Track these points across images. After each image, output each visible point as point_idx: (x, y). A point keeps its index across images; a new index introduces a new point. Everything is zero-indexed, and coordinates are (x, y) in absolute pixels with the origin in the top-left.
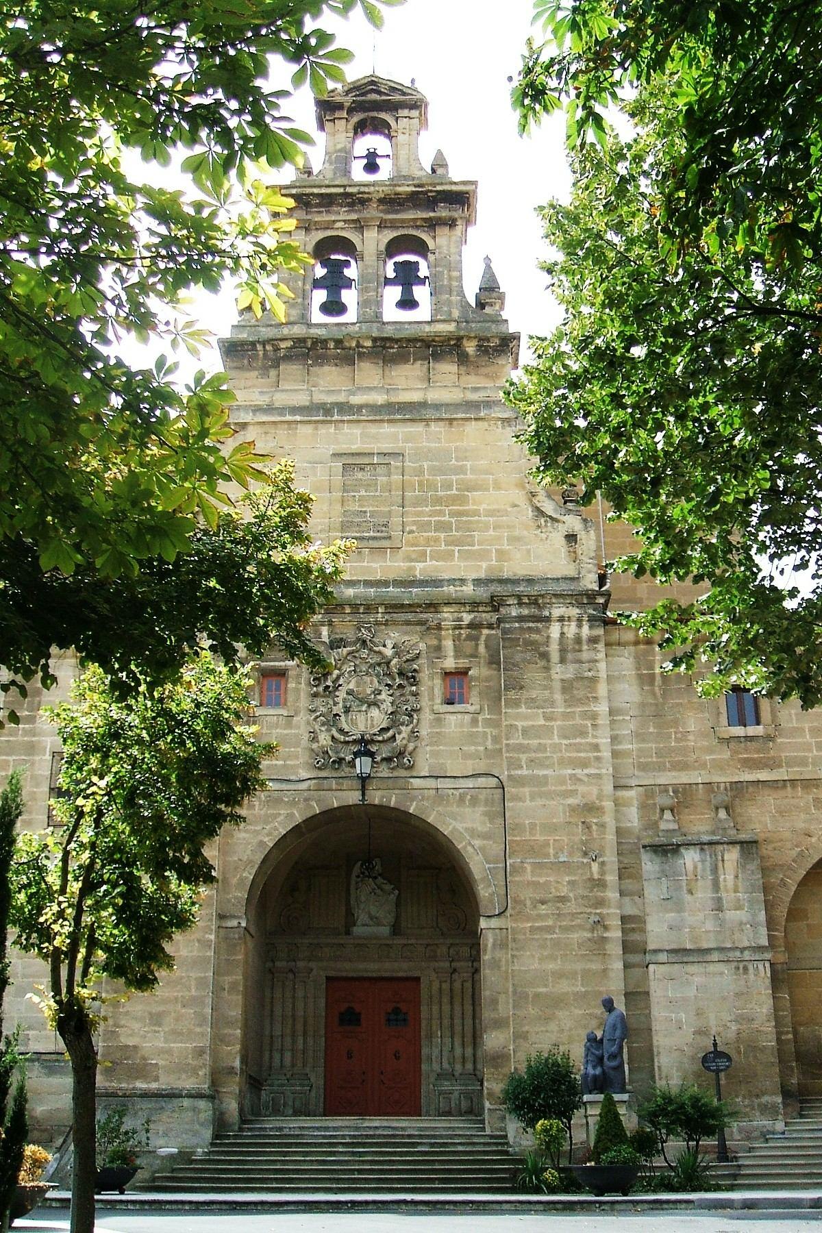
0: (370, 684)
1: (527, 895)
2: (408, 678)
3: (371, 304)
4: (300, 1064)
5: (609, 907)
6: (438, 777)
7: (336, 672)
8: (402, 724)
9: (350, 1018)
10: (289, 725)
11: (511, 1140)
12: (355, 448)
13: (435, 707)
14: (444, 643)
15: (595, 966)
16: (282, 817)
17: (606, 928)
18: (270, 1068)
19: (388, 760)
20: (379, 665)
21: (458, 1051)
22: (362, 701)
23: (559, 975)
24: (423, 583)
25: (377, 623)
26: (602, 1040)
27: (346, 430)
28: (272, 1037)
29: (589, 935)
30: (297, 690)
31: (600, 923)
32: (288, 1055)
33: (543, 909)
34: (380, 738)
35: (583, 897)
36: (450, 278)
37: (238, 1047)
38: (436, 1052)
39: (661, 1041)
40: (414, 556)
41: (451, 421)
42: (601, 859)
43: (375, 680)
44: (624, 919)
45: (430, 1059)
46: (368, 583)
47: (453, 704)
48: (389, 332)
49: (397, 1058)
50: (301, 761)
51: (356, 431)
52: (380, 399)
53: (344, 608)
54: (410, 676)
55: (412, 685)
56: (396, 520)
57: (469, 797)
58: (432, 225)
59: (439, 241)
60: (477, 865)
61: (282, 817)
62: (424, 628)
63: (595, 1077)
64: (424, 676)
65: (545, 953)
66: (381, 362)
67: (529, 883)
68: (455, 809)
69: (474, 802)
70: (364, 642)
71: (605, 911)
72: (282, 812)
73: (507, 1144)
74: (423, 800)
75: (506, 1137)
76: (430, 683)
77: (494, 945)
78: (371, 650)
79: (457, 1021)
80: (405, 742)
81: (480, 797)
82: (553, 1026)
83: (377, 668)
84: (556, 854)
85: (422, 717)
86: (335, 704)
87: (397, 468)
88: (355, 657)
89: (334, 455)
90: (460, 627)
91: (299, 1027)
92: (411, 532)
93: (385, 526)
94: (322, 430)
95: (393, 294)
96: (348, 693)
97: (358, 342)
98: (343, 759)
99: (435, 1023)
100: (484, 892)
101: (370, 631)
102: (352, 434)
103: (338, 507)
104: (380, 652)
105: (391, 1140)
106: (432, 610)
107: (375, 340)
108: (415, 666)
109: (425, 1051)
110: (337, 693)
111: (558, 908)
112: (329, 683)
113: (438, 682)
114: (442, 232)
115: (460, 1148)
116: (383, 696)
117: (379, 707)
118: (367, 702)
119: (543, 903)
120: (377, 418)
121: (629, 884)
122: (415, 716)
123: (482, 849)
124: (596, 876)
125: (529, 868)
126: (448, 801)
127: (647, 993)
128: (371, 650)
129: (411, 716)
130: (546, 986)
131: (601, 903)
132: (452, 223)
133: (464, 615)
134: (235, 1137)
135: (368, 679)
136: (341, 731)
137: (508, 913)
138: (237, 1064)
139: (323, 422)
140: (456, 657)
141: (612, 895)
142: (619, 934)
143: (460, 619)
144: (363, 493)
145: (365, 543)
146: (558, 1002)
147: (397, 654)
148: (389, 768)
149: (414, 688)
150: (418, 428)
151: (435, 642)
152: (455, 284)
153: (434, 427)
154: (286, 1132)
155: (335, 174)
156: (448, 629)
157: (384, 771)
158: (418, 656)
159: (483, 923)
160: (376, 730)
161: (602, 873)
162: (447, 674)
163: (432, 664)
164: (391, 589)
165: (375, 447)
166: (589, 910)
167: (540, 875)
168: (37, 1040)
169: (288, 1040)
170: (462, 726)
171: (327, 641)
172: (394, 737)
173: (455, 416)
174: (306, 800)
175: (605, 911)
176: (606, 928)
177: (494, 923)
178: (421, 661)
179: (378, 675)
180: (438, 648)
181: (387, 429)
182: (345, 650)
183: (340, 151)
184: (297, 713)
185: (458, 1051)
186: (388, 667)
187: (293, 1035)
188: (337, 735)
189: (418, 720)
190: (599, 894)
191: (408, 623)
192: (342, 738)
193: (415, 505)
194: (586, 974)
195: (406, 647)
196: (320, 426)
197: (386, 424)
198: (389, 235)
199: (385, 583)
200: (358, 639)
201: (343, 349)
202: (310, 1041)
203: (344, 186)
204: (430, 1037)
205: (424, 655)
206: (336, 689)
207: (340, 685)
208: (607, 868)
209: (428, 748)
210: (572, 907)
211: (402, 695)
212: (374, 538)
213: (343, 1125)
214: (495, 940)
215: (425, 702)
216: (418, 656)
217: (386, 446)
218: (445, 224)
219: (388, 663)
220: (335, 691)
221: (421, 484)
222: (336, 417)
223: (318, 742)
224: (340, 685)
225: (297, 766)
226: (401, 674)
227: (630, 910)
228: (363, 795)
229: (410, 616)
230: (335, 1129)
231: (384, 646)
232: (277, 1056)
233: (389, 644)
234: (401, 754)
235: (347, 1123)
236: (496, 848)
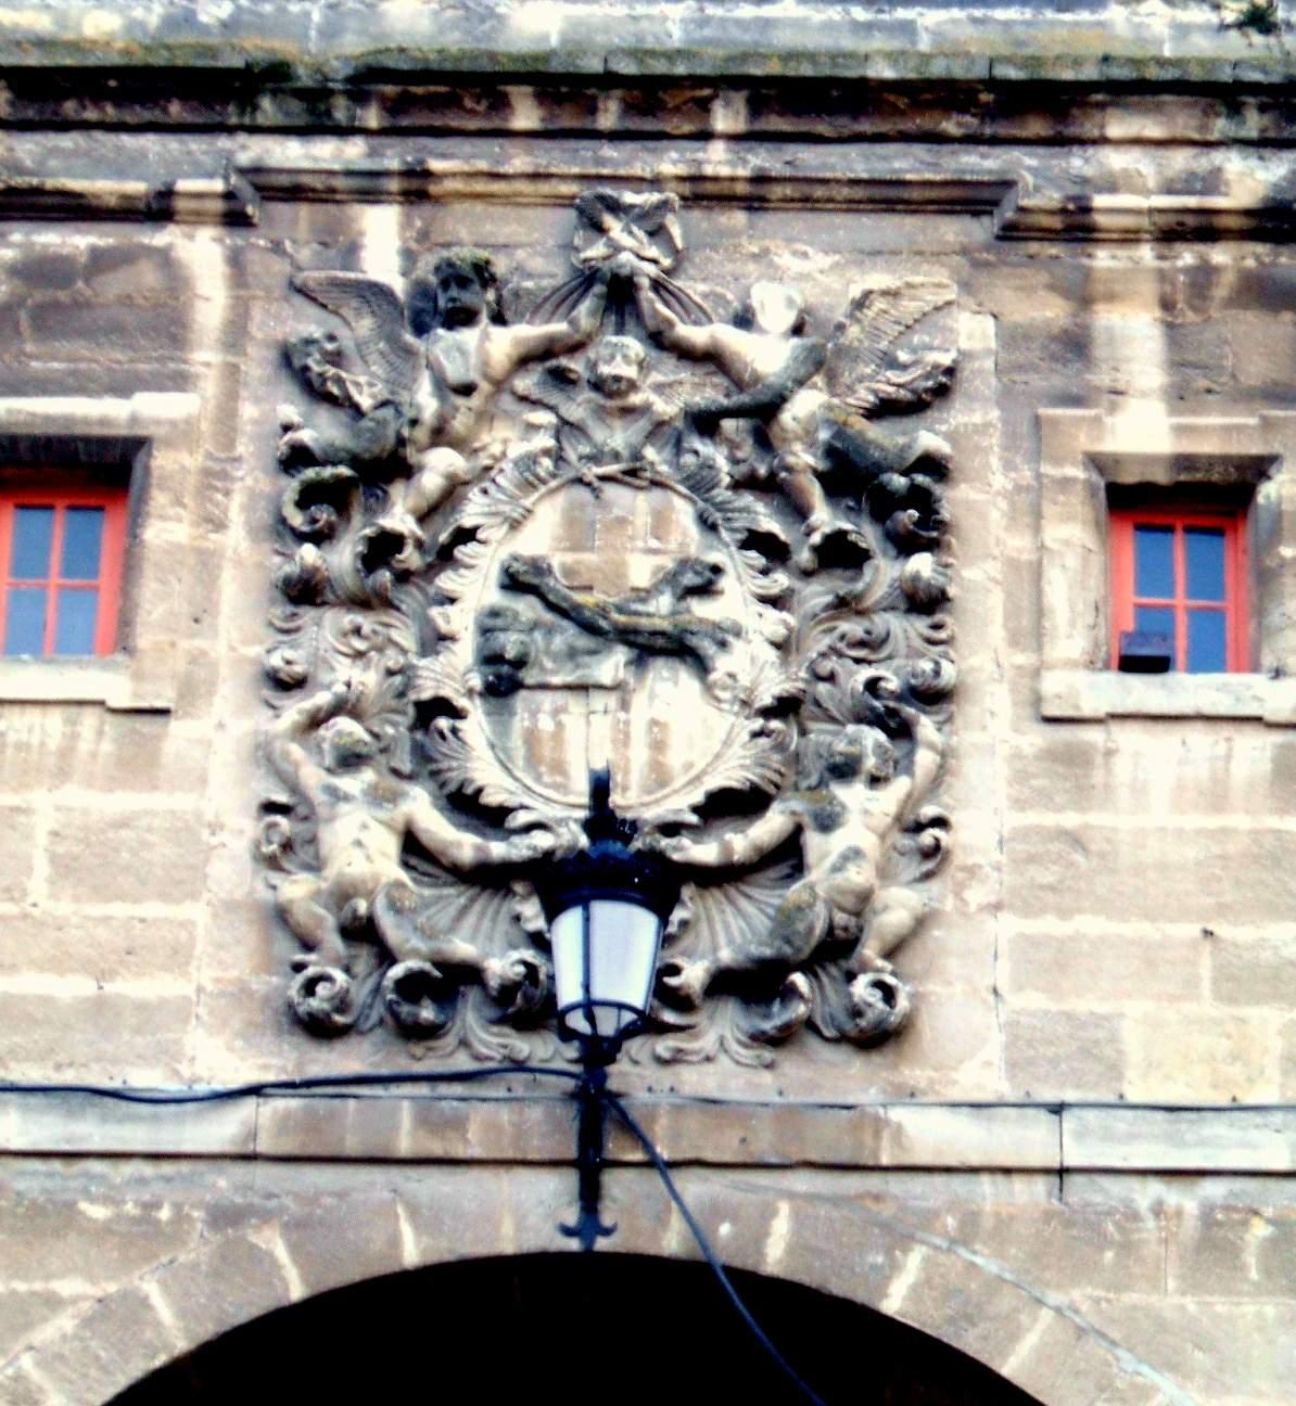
2: (881, 505)
6: (1007, 1171)
7: (438, 466)
8: (844, 770)
10: (138, 767)
13: (1052, 683)
14: (1107, 318)
16: (66, 1322)
25: (703, 194)
30: (206, 564)
34: (704, 852)
43: (683, 512)
47: (1158, 665)
50: (206, 976)
53: (501, 104)
55: (905, 545)
57: (1260, 1230)
61: (66, 1322)
62: (979, 230)
68: (1173, 1300)
72: (66, 1287)
76: (1019, 544)
78: (659, 340)
80: (858, 876)
83: (705, 448)
86: (436, 641)
88: (562, 378)
90: (1202, 228)
96: (514, 583)
98: (469, 974)
101: (657, 233)
104: (711, 359)
106: (1037, 127)
110: (446, 581)
112: (399, 517)
117: (701, 666)
118: (626, 636)
122: (926, 726)
126: (1127, 1247)
128: (659, 340)
129: (902, 731)
133: (1233, 163)
135: (637, 505)
136: (466, 805)
140: (1180, 396)
143: (1212, 182)
147: (819, 364)
148: (759, 1039)
149: (922, 564)
151: (1052, 311)
156: (1129, 238)
160: (680, 803)
163: (1036, 437)
170: (1216, 796)
174: (225, 1217)
179: (699, 484)
180: (1075, 345)
182: (498, 344)
184: (193, 691)
188: (440, 828)
189: (944, 754)
191: (887, 197)
192: (465, 844)
195: (875, 333)
200: (587, 278)
205: (981, 378)
206: (445, 557)
207: (466, 535)
209: (1008, 926)
211: (844, 605)
216: (940, 390)
219: (764, 413)
220: (431, 571)
223: (315, 866)
224: (466, 535)
225: (182, 1012)
228: (590, 1196)
229: (906, 163)
233: (775, 308)
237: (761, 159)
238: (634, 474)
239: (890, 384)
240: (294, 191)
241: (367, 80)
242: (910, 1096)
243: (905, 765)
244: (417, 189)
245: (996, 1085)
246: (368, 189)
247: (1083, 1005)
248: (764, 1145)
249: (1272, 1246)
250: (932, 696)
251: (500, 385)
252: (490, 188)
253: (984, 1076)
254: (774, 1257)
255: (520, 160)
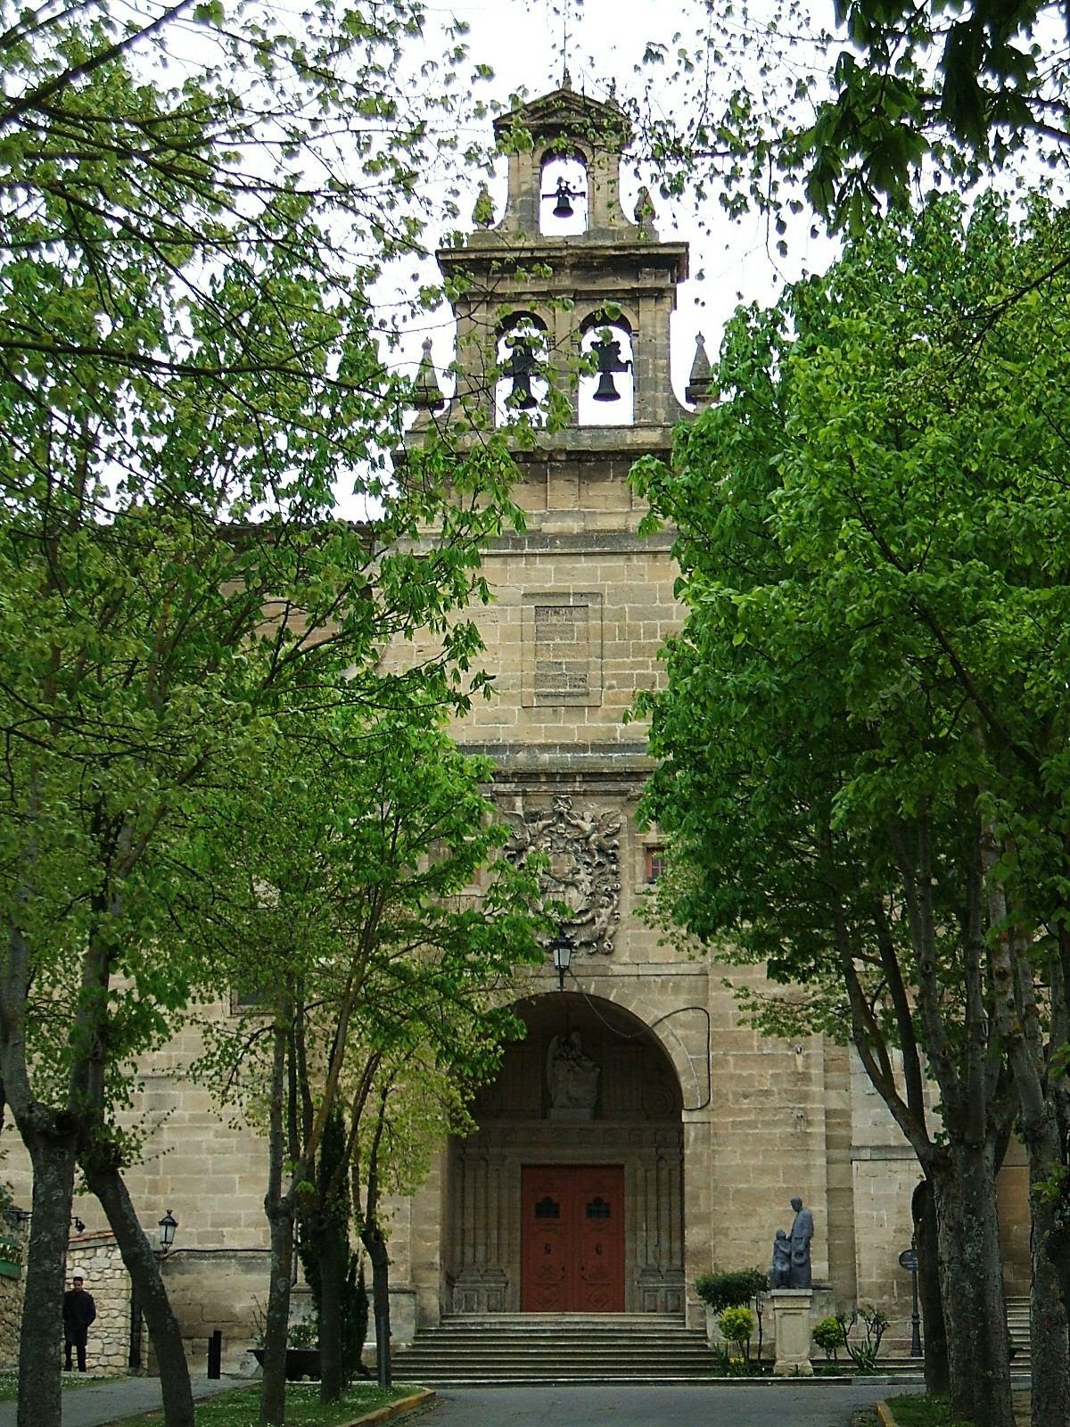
0: (566, 864)
1: (729, 1088)
2: (608, 855)
3: (562, 405)
4: (494, 1260)
5: (814, 1102)
8: (602, 906)
9: (547, 1209)
11: (710, 1335)
12: (548, 586)
15: (797, 1162)
17: (809, 1123)
18: (462, 1263)
19: (587, 944)
20: (577, 841)
21: (665, 1245)
22: (559, 882)
23: (762, 1171)
24: (623, 747)
25: (575, 793)
26: (790, 1238)
27: (538, 565)
28: (463, 1231)
29: (790, 1130)
31: (804, 1119)
32: (481, 1249)
33: (745, 1103)
34: (579, 921)
35: (786, 1091)
36: (655, 368)
37: (438, 1243)
38: (641, 1246)
39: (861, 1238)
40: (614, 716)
41: (655, 553)
42: (805, 1052)
44: (828, 1113)
45: (634, 1251)
46: (565, 748)
48: (586, 442)
49: (599, 1252)
51: (550, 565)
52: (575, 526)
54: (609, 854)
55: (612, 863)
56: (595, 673)
58: (634, 296)
59: (645, 316)
60: (680, 1058)
62: (625, 798)
63: (782, 1273)
64: (624, 853)
65: (747, 1149)
66: (576, 480)
67: (732, 1077)
68: (657, 997)
69: (677, 989)
70: (561, 814)
71: (809, 1106)
73: (706, 1338)
74: (623, 986)
75: (705, 1331)
76: (630, 860)
77: (696, 1139)
78: (568, 823)
79: (664, 1213)
81: (683, 984)
82: (753, 1222)
84: (760, 1048)
85: (622, 897)
87: (595, 611)
89: (525, 595)
91: (493, 1220)
92: (611, 687)
93: (583, 680)
94: (513, 565)
95: (590, 385)
97: (550, 455)
99: (640, 1214)
100: (688, 1084)
102: (545, 570)
103: (531, 658)
104: (578, 826)
105: (594, 1333)
107: (569, 453)
108: (616, 842)
109: (628, 1245)
111: (761, 1103)
113: (640, 858)
114: (647, 306)
115: (660, 1342)
116: (581, 876)
119: (746, 1097)
120: (573, 551)
121: (835, 1077)
123: (685, 1038)
124: (801, 1070)
125: (731, 1059)
127: (851, 1190)
129: (611, 897)
130: (748, 1182)
131: (805, 1097)
132: (658, 294)
134: (437, 1331)
137: (711, 1105)
138: (437, 1259)
139: (511, 555)
141: (816, 1089)
142: (823, 1129)
144: (558, 641)
145: (560, 701)
146: (758, 1198)
149: (614, 867)
150: (618, 563)
152: (661, 375)
153: (635, 560)
154: (487, 1326)
155: (520, 225)
157: (582, 958)
158: (618, 830)
159: (685, 1117)
161: (807, 1066)
162: (650, 849)
163: (633, 839)
164: (589, 754)
165: (571, 585)
166: (791, 1105)
167: (743, 1068)
168: (232, 1236)
169: (481, 1233)
171: (521, 813)
172: (592, 921)
173: (660, 548)
175: (809, 1106)
176: (809, 1123)
177: (696, 1116)
178: (622, 835)
179: (576, 852)
181: (584, 563)
182: (541, 824)
183: (526, 193)
185: (665, 1245)
186: (587, 843)
187: (487, 1229)
190: (804, 1088)
191: (608, 793)
193: (614, 655)
194: (788, 1170)
196: (509, 560)
197: (583, 558)
198: (586, 310)
199: (583, 748)
201: (532, 462)
202: (505, 1234)
203: (532, 250)
204: (635, 1230)
208: (812, 1060)
209: (629, 931)
210: (774, 1101)
212: (570, 695)
213: (545, 1320)
214: (696, 1135)
215: (625, 882)
216: (618, 830)
217: (583, 585)
218: (651, 297)
219: (587, 838)
221: (621, 629)
222: (527, 550)
226: (601, 850)
227: (836, 1103)
229: (610, 787)
230: (535, 1323)
231: (583, 819)
232: (469, 1251)
233: (587, 815)
234: (600, 938)
235: (549, 1319)
236: (698, 1038)
237: (585, 786)
238: (565, 851)
239: (609, 831)
240: (503, 794)
241: (514, 774)
242: (614, 963)
243: (611, 904)
244: (525, 794)
245: (628, 960)
246: (516, 794)
247: (643, 946)
248: (590, 972)
249: (673, 987)
250: (616, 891)
251: (541, 832)
252: (537, 794)
253: (625, 959)
254: (592, 991)
255: (544, 788)
